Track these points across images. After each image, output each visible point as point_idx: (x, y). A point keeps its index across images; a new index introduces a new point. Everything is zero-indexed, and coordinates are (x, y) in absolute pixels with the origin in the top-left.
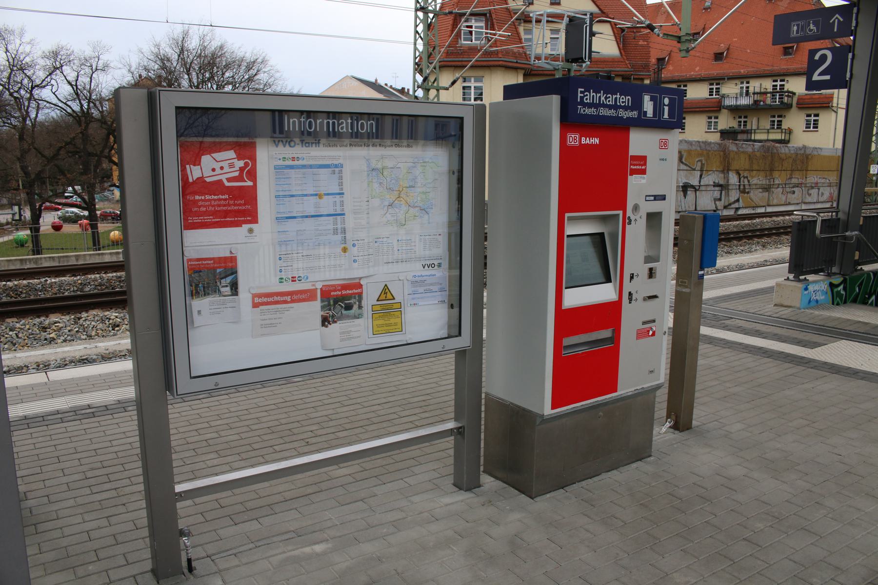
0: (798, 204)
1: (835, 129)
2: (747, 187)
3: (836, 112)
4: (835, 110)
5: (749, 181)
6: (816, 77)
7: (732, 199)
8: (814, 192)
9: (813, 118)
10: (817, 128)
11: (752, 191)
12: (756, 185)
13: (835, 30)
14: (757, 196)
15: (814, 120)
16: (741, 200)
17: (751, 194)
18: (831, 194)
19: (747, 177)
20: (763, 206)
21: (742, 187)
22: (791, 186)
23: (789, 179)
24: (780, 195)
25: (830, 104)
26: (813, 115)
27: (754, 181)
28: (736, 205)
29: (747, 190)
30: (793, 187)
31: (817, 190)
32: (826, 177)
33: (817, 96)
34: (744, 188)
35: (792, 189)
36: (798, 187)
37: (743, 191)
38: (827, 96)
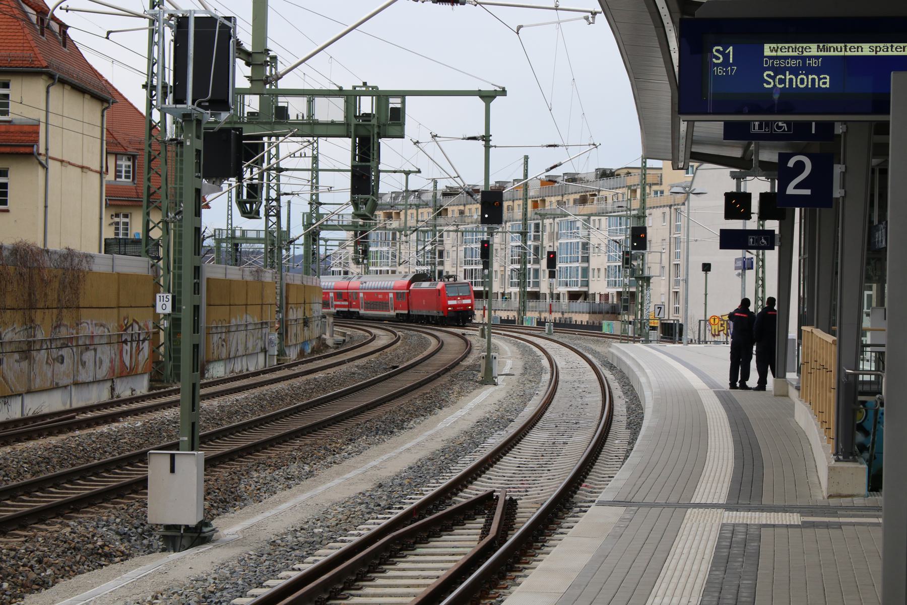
0: (66, 387)
1: (46, 207)
3: (45, 167)
4: (44, 162)
6: (790, 190)
8: (88, 356)
11: (5, 359)
12: (11, 342)
13: (813, 132)
18: (111, 362)
20: (20, 395)
22: (59, 343)
23: (55, 328)
24: (45, 367)
25: (35, 149)
27: (8, 336)
30: (62, 348)
31: (93, 352)
32: (104, 322)
33: (3, 128)
35: (60, 353)
36: (67, 346)
38: (26, 129)
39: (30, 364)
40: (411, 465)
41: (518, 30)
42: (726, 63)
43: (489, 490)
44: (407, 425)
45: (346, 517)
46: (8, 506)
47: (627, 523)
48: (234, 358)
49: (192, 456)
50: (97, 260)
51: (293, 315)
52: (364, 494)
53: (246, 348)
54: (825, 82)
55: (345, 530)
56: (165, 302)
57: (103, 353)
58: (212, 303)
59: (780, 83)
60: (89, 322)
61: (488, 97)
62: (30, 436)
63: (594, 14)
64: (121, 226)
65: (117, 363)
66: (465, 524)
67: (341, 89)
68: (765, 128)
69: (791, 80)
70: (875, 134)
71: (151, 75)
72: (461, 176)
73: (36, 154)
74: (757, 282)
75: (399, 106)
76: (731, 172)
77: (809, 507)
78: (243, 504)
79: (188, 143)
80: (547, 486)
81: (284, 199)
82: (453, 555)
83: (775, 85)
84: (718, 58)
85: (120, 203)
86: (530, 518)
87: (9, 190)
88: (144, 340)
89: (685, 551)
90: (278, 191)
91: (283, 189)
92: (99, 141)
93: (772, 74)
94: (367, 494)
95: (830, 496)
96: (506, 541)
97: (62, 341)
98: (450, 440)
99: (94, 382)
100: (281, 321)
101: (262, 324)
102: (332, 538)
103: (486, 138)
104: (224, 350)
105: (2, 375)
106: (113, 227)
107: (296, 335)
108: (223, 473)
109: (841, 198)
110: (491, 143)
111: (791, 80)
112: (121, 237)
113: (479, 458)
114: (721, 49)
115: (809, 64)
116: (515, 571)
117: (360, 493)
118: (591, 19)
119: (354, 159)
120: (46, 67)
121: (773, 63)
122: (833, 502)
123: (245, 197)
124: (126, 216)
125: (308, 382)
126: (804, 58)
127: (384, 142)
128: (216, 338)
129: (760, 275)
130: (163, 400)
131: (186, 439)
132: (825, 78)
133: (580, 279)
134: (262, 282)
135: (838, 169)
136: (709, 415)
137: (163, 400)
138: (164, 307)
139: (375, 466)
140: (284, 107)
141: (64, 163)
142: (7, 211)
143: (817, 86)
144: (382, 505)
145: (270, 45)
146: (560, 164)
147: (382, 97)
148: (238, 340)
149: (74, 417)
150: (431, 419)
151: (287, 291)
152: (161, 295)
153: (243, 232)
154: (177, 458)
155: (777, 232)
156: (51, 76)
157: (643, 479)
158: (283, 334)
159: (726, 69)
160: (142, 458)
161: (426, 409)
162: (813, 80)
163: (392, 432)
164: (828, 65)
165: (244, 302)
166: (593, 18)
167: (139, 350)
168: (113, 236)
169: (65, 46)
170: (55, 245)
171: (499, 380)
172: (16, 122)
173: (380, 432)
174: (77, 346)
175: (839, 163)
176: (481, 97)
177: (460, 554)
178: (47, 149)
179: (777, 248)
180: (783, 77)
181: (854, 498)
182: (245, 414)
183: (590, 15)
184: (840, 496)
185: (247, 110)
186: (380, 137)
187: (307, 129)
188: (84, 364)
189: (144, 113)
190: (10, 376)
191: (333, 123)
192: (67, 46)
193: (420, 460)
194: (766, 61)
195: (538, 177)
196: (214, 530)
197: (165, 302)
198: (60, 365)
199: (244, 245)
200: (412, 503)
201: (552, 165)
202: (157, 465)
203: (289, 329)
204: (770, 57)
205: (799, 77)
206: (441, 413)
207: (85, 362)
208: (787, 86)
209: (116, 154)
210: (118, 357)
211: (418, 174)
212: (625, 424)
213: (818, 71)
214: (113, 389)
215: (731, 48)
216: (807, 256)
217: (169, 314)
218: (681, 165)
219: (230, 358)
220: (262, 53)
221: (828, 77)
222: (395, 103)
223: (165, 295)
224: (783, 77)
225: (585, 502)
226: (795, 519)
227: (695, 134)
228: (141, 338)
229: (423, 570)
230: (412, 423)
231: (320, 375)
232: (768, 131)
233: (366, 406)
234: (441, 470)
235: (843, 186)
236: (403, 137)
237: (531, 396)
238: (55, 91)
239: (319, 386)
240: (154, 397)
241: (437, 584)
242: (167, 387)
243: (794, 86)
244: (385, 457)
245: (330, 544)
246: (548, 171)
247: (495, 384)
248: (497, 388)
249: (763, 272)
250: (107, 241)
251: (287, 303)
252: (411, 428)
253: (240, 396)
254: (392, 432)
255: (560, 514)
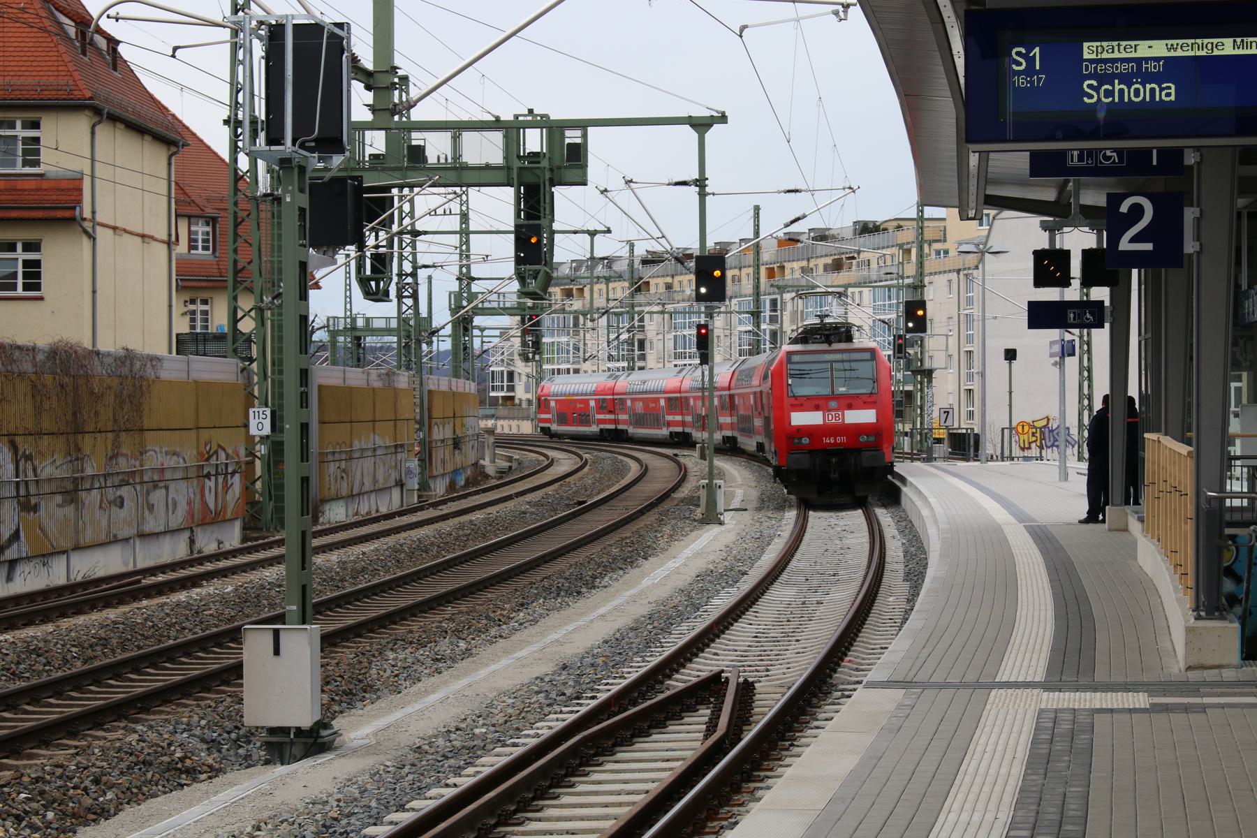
0: (127, 540)
1: (94, 292)
2: (33, 490)
3: (92, 237)
4: (90, 230)
5: (35, 470)
6: (1125, 245)
7: (6, 535)
8: (158, 496)
9: (21, 255)
10: (37, 287)
11: (43, 503)
12: (50, 480)
13: (1155, 163)
14: (53, 513)
15: (27, 263)
16: (22, 534)
17: (42, 512)
18: (189, 503)
19: (29, 458)
20: (64, 552)
21: (22, 492)
22: (116, 480)
23: (111, 458)
24: (98, 513)
25: (77, 212)
26: (19, 247)
27: (47, 470)
28: (10, 554)
29: (33, 501)
30: (120, 486)
31: (163, 491)
32: (178, 450)
33: (32, 184)
34: (28, 495)
35: (118, 493)
37: (27, 506)
38: (64, 185)
39: (77, 509)
40: (607, 637)
41: (741, 31)
42: (1030, 70)
43: (716, 669)
44: (600, 583)
45: (518, 711)
46: (51, 705)
47: (908, 711)
48: (359, 495)
49: (304, 634)
50: (166, 364)
51: (438, 434)
52: (542, 679)
53: (375, 481)
54: (1168, 93)
55: (518, 729)
56: (261, 420)
57: (177, 491)
58: (326, 420)
59: (1106, 97)
60: (157, 450)
61: (701, 125)
62: (78, 609)
63: (846, 7)
64: (199, 317)
65: (197, 505)
66: (683, 718)
67: (498, 119)
68: (1087, 160)
69: (1121, 91)
70: (1242, 163)
71: (235, 105)
72: (667, 236)
73: (78, 218)
74: (1081, 373)
75: (579, 141)
76: (1042, 222)
77: (1160, 684)
78: (375, 697)
79: (288, 199)
80: (796, 662)
81: (422, 274)
82: (668, 760)
83: (1099, 99)
84: (1019, 64)
85: (196, 284)
86: (773, 707)
87: (42, 270)
88: (233, 473)
89: (989, 748)
90: (414, 262)
91: (421, 260)
92: (165, 199)
93: (1095, 83)
94: (547, 679)
95: (1189, 668)
96: (740, 740)
97: (120, 477)
98: (660, 602)
99: (165, 533)
100: (422, 443)
101: (396, 446)
102: (499, 741)
103: (701, 183)
104: (345, 484)
105: (40, 526)
106: (187, 318)
107: (443, 462)
108: (346, 654)
109: (1195, 254)
110: (708, 190)
111: (1121, 91)
112: (198, 330)
113: (700, 625)
114: (1023, 51)
115: (1147, 68)
116: (754, 781)
117: (537, 678)
118: (842, 14)
119: (518, 215)
120: (91, 98)
121: (1096, 68)
122: (1194, 676)
123: (368, 272)
124: (205, 302)
125: (462, 526)
126: (1138, 61)
127: (558, 191)
128: (332, 468)
129: (1086, 364)
130: (262, 555)
131: (294, 608)
132: (1169, 88)
133: (505, 384)
134: (395, 389)
135: (1190, 214)
136: (1019, 560)
137: (262, 555)
138: (260, 426)
139: (557, 641)
140: (419, 146)
141: (117, 231)
142: (41, 299)
143: (1157, 99)
144: (568, 694)
145: (397, 62)
146: (804, 216)
147: (554, 129)
148: (363, 471)
149: (139, 581)
150: (633, 573)
151: (430, 401)
152: (256, 410)
153: (368, 320)
154: (282, 634)
155: (1107, 303)
156: (97, 111)
157: (927, 650)
158: (426, 459)
159: (1031, 78)
160: (235, 635)
161: (625, 560)
162: (1152, 90)
163: (579, 593)
164: (1172, 69)
165: (370, 417)
166: (845, 12)
167: (227, 488)
168: (186, 330)
169: (115, 69)
170: (107, 344)
171: (727, 517)
172: (49, 175)
173: (562, 594)
174: (142, 483)
175: (1192, 205)
176: (693, 126)
177: (678, 760)
178: (94, 212)
179: (1107, 325)
180: (1110, 88)
181: (1222, 670)
182: (375, 572)
183: (840, 8)
184: (1203, 667)
185: (369, 151)
186: (553, 184)
187: (451, 176)
188: (151, 508)
189: (227, 160)
190: (51, 528)
191: (488, 167)
192: (119, 69)
193: (618, 630)
194: (1087, 66)
195: (774, 235)
196: (335, 733)
197: (261, 420)
198: (118, 510)
199: (368, 339)
200: (609, 690)
201: (793, 218)
202: (256, 645)
203: (434, 453)
204: (1091, 61)
205: (1133, 87)
206: (646, 565)
207: (153, 505)
208: (1117, 100)
209: (189, 217)
210: (198, 497)
211: (607, 235)
212: (901, 574)
213: (1158, 78)
214: (192, 541)
215: (1037, 50)
216: (1149, 335)
217: (268, 437)
218: (972, 213)
219: (351, 496)
220: (387, 71)
221: (1173, 86)
222: (572, 136)
223: (261, 410)
224: (1110, 88)
225: (848, 684)
226: (1140, 700)
227: (990, 170)
228: (230, 470)
229: (626, 782)
230: (607, 579)
231: (478, 516)
232: (1092, 163)
233: (543, 557)
234: (648, 643)
235: (1198, 237)
236: (585, 184)
237: (771, 538)
238: (104, 132)
239: (477, 531)
240: (249, 550)
241: (647, 801)
242: (267, 537)
243: (1126, 100)
244: (570, 627)
245: (497, 750)
246: (787, 226)
247: (721, 523)
248: (723, 528)
249: (1089, 359)
250: (181, 338)
251: (430, 418)
252: (605, 587)
253: (368, 547)
254: (579, 593)
255: (815, 701)
